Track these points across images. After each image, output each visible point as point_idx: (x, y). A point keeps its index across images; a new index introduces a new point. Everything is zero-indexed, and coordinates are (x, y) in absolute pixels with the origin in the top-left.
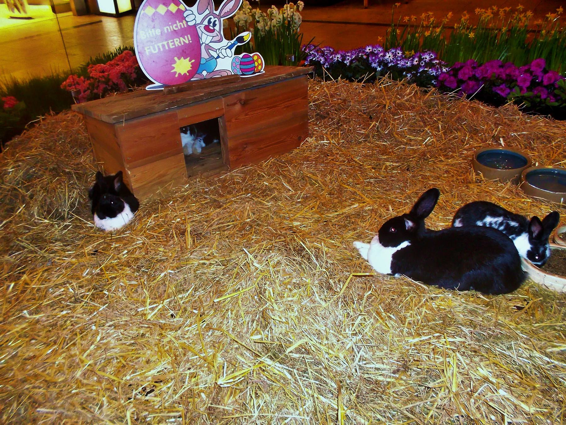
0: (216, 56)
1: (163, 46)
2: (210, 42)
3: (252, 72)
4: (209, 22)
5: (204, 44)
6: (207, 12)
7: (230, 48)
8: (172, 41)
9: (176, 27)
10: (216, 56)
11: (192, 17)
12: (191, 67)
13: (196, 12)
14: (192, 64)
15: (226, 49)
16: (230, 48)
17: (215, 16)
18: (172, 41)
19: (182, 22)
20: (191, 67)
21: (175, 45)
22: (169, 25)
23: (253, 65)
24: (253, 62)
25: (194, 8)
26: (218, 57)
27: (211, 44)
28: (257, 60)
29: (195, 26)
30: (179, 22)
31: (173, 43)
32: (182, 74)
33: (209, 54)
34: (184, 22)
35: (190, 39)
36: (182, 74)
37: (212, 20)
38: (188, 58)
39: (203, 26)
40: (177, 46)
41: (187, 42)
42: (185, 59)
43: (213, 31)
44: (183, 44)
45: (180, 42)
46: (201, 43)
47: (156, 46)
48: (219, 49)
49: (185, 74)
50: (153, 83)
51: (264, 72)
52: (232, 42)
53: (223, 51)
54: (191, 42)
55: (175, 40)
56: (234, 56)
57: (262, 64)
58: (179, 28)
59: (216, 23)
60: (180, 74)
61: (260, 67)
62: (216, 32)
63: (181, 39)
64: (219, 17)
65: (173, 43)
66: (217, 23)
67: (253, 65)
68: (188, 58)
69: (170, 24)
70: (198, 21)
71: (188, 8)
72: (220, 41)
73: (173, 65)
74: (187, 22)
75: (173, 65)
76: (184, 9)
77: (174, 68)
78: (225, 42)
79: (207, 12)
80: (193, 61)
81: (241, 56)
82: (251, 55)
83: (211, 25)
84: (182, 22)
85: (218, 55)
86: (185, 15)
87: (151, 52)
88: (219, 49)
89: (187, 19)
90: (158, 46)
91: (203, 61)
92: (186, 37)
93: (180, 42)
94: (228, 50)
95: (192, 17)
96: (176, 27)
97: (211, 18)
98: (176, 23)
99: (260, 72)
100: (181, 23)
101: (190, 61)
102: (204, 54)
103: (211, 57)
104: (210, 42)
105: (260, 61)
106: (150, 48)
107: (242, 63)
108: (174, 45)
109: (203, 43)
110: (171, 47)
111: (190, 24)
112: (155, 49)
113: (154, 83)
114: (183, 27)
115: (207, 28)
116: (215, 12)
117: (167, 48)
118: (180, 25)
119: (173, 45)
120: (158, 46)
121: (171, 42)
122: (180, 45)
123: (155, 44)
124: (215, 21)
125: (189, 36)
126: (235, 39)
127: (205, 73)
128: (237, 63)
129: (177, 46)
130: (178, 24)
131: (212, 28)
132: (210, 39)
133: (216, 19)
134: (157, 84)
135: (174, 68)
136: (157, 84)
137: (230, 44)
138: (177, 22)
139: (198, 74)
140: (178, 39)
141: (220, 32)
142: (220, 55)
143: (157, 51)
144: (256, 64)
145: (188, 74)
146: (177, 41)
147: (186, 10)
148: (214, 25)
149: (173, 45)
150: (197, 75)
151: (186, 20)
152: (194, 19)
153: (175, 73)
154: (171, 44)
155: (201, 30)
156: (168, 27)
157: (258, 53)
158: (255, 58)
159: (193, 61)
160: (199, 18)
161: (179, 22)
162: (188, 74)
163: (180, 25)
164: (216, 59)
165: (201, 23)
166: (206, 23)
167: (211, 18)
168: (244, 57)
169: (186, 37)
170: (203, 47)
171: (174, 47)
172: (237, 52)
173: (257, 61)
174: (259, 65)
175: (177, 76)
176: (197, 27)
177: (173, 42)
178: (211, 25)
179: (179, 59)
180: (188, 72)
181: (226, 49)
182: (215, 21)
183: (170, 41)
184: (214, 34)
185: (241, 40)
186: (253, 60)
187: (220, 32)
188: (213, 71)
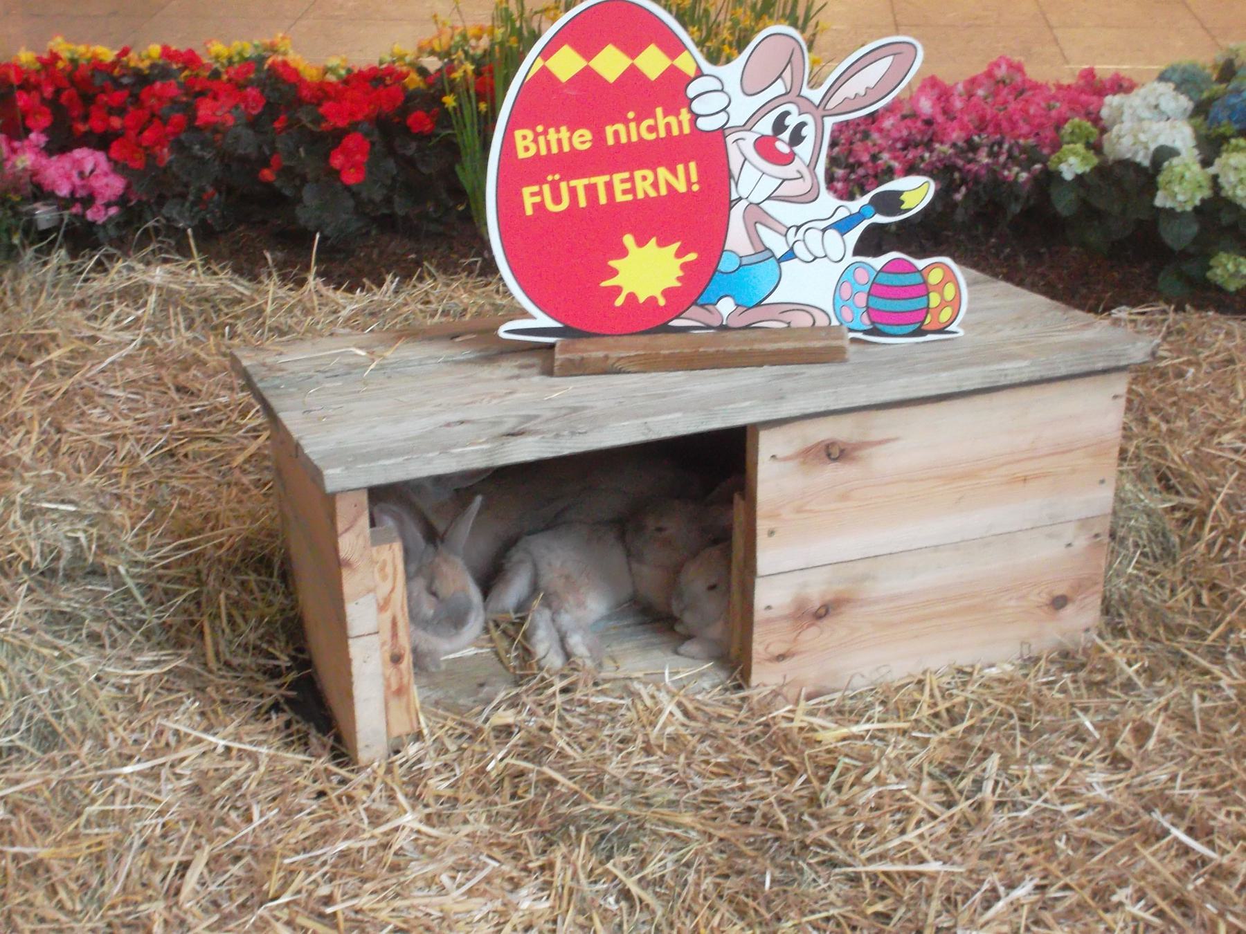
0: (780, 250)
1: (591, 190)
2: (769, 198)
3: (911, 328)
4: (779, 126)
5: (743, 204)
6: (778, 88)
7: (843, 227)
8: (626, 175)
9: (652, 129)
10: (780, 249)
11: (720, 100)
12: (679, 279)
13: (733, 86)
14: (684, 267)
15: (824, 230)
16: (843, 227)
17: (805, 105)
20: (679, 279)
21: (635, 195)
22: (626, 122)
23: (918, 304)
24: (923, 289)
25: (731, 72)
26: (790, 255)
27: (769, 206)
28: (943, 283)
29: (721, 132)
30: (665, 116)
32: (642, 299)
33: (754, 237)
34: (685, 116)
35: (694, 178)
36: (642, 299)
37: (791, 122)
38: (675, 247)
39: (751, 137)
40: (640, 195)
41: (681, 187)
42: (662, 243)
43: (788, 159)
44: (663, 191)
45: (655, 185)
46: (734, 196)
47: (563, 186)
48: (798, 228)
49: (652, 300)
50: (524, 314)
51: (961, 333)
52: (855, 206)
53: (813, 237)
55: (638, 174)
56: (850, 259)
57: (956, 303)
58: (663, 134)
59: (804, 132)
60: (632, 297)
61: (945, 315)
62: (797, 164)
63: (663, 172)
64: (821, 110)
65: (628, 186)
66: (808, 132)
67: (918, 304)
68: (675, 247)
69: (631, 115)
70: (738, 119)
71: (707, 67)
72: (810, 197)
73: (613, 263)
74: (695, 117)
75: (613, 263)
76: (691, 72)
77: (614, 273)
78: (828, 205)
79: (778, 88)
80: (692, 257)
81: (879, 262)
82: (921, 264)
83: (786, 136)
84: (677, 114)
85: (792, 249)
86: (692, 91)
87: (539, 207)
88: (798, 228)
89: (697, 107)
90: (573, 192)
91: (727, 264)
92: (680, 168)
93: (655, 185)
94: (832, 234)
95: (720, 100)
96: (652, 129)
97: (787, 114)
98: (654, 117)
99: (941, 331)
100: (672, 119)
101: (679, 254)
102: (737, 239)
103: (765, 252)
104: (769, 198)
105: (949, 292)
106: (540, 193)
107: (877, 289)
108: (633, 191)
109: (740, 199)
110: (620, 198)
111: (703, 124)
112: (557, 199)
113: (532, 317)
115: (765, 147)
116: (806, 92)
117: (603, 199)
118: (668, 126)
119: (625, 192)
120: (573, 192)
121: (623, 181)
122: (652, 194)
123: (561, 180)
124: (803, 124)
125: (692, 165)
126: (866, 199)
127: (726, 307)
128: (857, 288)
129: (640, 195)
130: (661, 123)
131: (783, 147)
132: (769, 185)
133: (807, 118)
134: (544, 321)
135: (614, 273)
136: (544, 321)
137: (842, 214)
138: (659, 111)
139: (702, 306)
140: (649, 173)
141: (812, 166)
142: (799, 249)
144: (934, 300)
145: (662, 302)
146: (644, 178)
147: (700, 74)
148: (797, 138)
149: (625, 192)
150: (693, 308)
151: (690, 111)
152: (724, 110)
153: (617, 290)
154: (618, 188)
155: (740, 150)
156: (620, 127)
157: (947, 260)
158: (935, 277)
159: (692, 257)
160: (742, 109)
161: (665, 116)
162: (662, 302)
163: (668, 126)
164: (779, 261)
165: (747, 126)
166: (765, 127)
167: (787, 114)
168: (885, 269)
170: (737, 213)
171: (629, 197)
172: (872, 243)
173: (940, 287)
174: (944, 304)
175: (619, 302)
176: (730, 140)
178: (786, 136)
179: (641, 242)
180: (667, 293)
181: (824, 230)
182: (803, 124)
183: (617, 178)
184: (789, 171)
185: (890, 202)
186: (925, 282)
187: (812, 166)
188: (758, 305)
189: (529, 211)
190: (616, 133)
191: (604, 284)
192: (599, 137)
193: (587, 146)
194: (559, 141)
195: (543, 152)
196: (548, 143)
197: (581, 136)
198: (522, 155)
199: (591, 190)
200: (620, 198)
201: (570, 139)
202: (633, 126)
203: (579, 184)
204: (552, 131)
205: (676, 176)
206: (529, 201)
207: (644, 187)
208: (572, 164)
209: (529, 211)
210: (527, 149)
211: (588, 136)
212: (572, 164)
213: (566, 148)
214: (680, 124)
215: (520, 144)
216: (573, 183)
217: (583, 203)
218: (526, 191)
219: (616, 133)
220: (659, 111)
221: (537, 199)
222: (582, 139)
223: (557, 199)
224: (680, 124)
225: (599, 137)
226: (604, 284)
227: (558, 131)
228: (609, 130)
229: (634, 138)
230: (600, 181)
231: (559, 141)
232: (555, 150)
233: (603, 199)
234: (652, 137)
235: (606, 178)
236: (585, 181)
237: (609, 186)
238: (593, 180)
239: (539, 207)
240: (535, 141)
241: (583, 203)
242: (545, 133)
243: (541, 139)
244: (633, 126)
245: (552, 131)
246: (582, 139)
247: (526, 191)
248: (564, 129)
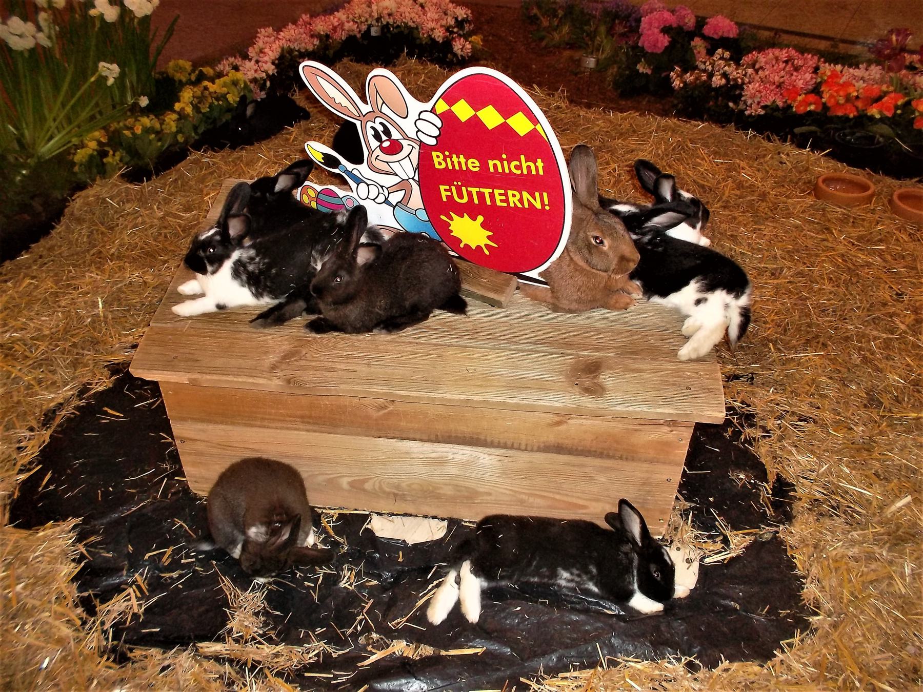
9: (517, 167)
18: (502, 191)
19: (535, 162)
22: (502, 161)
31: (504, 198)
35: (546, 202)
40: (512, 205)
41: (538, 205)
44: (526, 206)
47: (464, 189)
54: (547, 208)
55: (510, 193)
58: (525, 172)
63: (526, 195)
65: (504, 198)
84: (535, 162)
87: (450, 198)
90: (470, 194)
92: (537, 194)
93: (521, 200)
96: (517, 167)
106: (450, 190)
108: (507, 201)
112: (461, 196)
114: (534, 172)
117: (489, 202)
118: (529, 167)
119: (502, 201)
120: (470, 194)
121: (500, 194)
122: (519, 205)
123: (462, 185)
125: (545, 195)
130: (524, 165)
138: (523, 157)
143: (465, 200)
149: (502, 201)
154: (498, 198)
163: (529, 167)
169: (537, 194)
171: (505, 204)
177: (506, 195)
183: (497, 192)
189: (445, 199)
190: (495, 166)
191: (496, 246)
192: (484, 166)
193: (477, 169)
194: (459, 163)
195: (450, 167)
196: (452, 162)
197: (473, 163)
198: (437, 166)
199: (481, 196)
200: (499, 203)
201: (466, 163)
202: (505, 163)
203: (474, 190)
204: (454, 156)
205: (535, 199)
206: (444, 194)
207: (513, 200)
208: (468, 178)
209: (445, 199)
210: (440, 164)
211: (477, 164)
212: (468, 178)
213: (464, 168)
214: (537, 168)
215: (436, 160)
216: (469, 189)
217: (476, 201)
218: (442, 188)
219: (495, 166)
220: (523, 157)
221: (449, 193)
222: (474, 165)
223: (461, 196)
224: (537, 168)
225: (484, 166)
226: (496, 246)
227: (458, 157)
228: (491, 163)
229: (507, 171)
230: (487, 191)
231: (459, 163)
232: (457, 168)
233: (489, 202)
234: (519, 172)
235: (490, 191)
236: (478, 190)
237: (492, 195)
238: (482, 190)
239: (450, 198)
240: (445, 160)
241: (476, 201)
242: (451, 157)
243: (448, 159)
244: (505, 163)
245: (454, 156)
246: (474, 165)
247: (442, 188)
248: (462, 156)
